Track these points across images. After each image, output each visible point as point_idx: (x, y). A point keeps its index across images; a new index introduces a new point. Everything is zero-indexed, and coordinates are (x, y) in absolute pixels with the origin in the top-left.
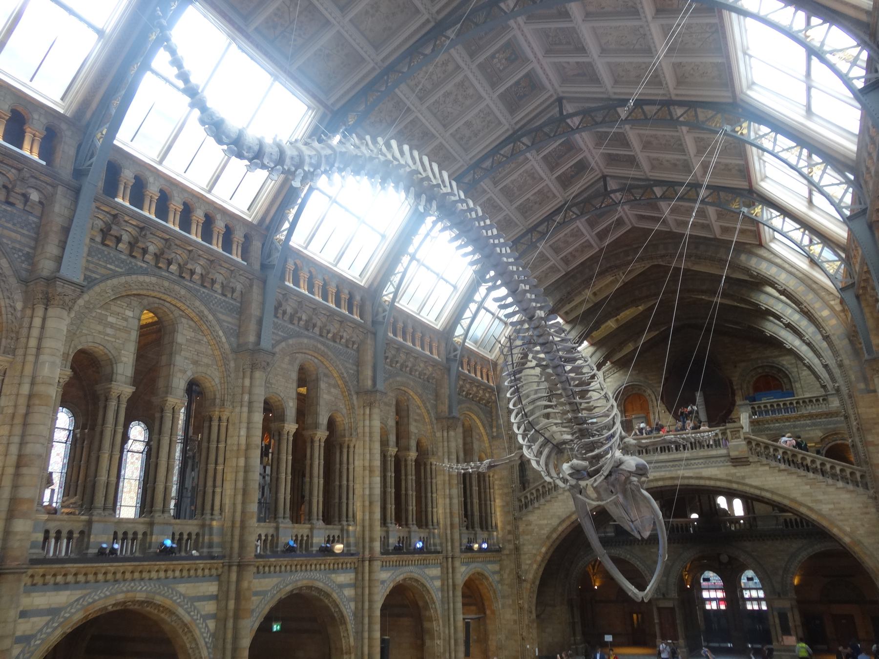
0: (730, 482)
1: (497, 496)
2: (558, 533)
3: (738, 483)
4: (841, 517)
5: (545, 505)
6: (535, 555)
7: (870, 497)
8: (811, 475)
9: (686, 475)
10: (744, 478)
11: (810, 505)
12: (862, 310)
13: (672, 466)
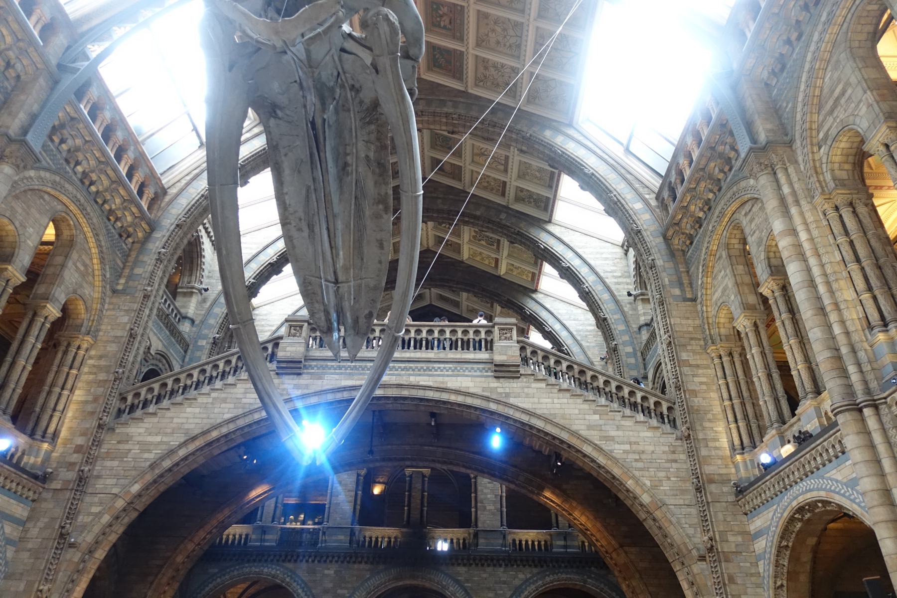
0: (487, 399)
1: (79, 385)
2: (176, 459)
3: (498, 402)
4: (640, 465)
5: (169, 409)
8: (603, 401)
9: (421, 383)
10: (508, 395)
11: (596, 442)
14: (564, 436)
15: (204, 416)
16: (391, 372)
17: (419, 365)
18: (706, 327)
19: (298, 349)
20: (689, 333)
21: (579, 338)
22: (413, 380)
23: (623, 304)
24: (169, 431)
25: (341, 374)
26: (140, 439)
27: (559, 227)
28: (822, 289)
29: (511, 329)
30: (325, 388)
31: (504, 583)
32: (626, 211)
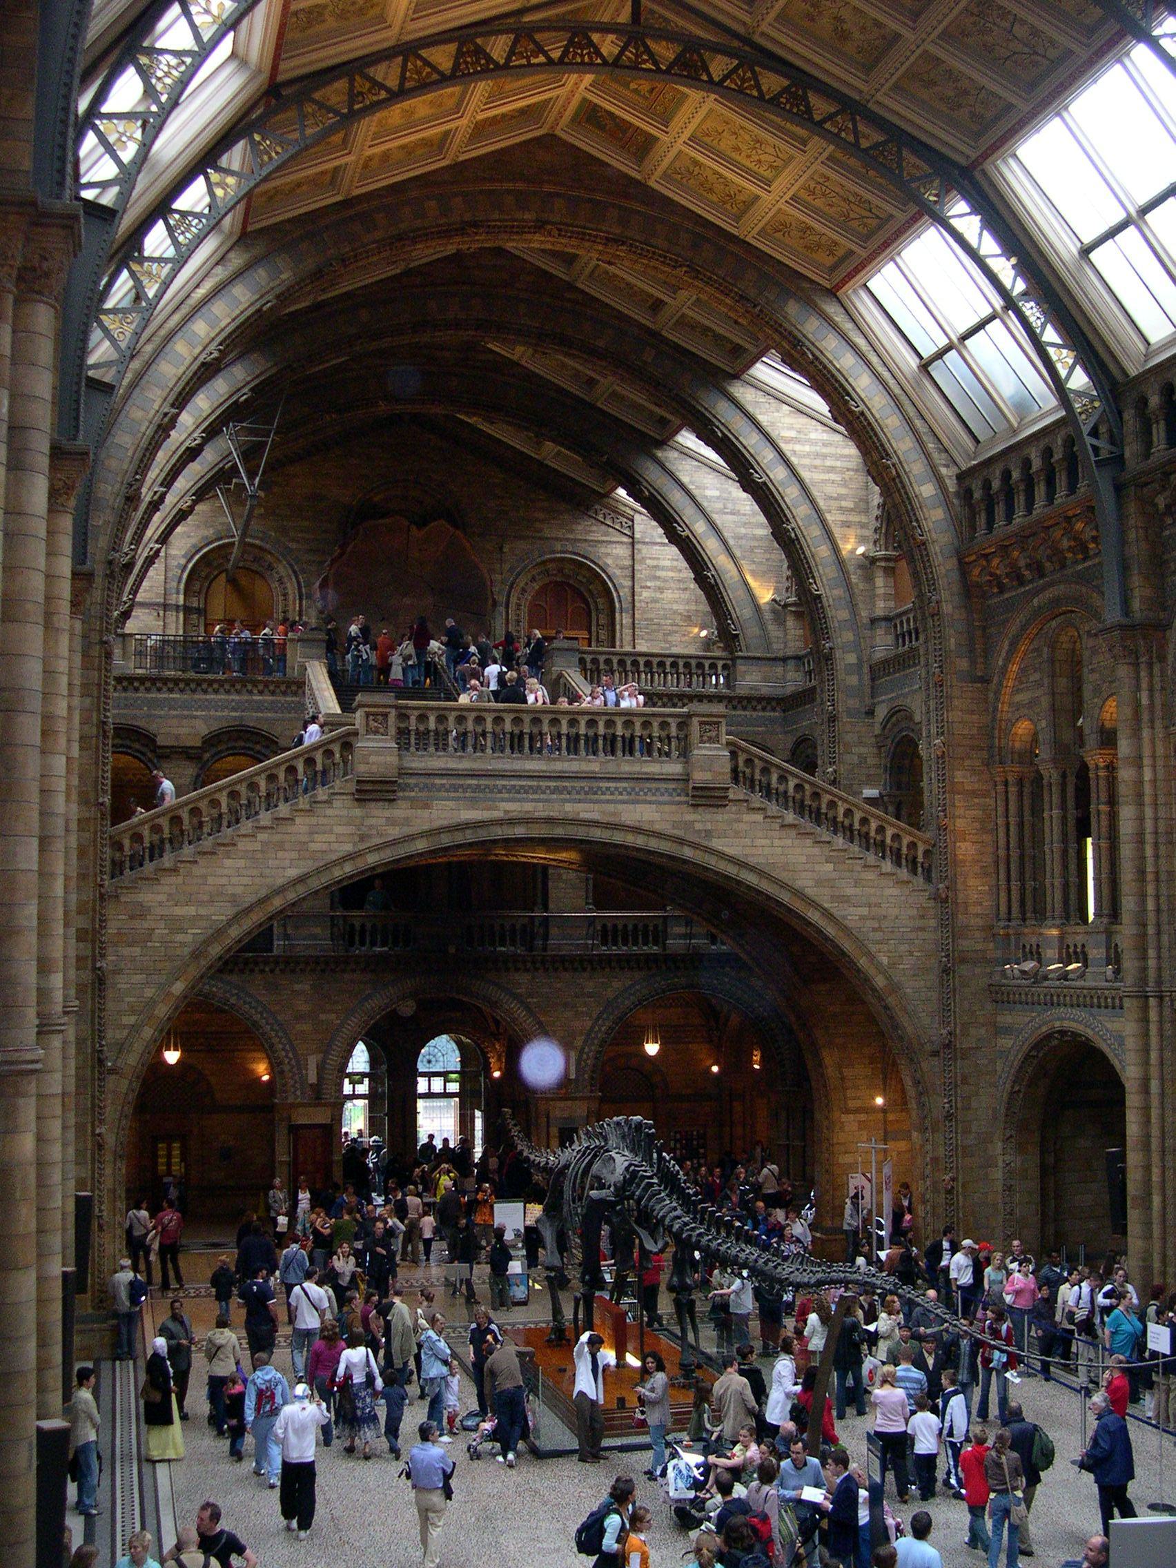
0: (681, 841)
4: (878, 936)
6: (152, 1003)
7: (936, 897)
8: (839, 841)
9: (583, 815)
10: (708, 834)
11: (826, 905)
12: (1121, 517)
13: (555, 790)
14: (785, 897)
15: (255, 872)
16: (535, 796)
17: (578, 784)
18: (996, 732)
19: (388, 759)
20: (972, 737)
21: (738, 553)
22: (568, 807)
23: (851, 569)
24: (206, 898)
25: (458, 799)
26: (166, 912)
27: (753, 390)
28: (1149, 851)
29: (718, 723)
30: (437, 824)
31: (590, 995)
32: (908, 498)
